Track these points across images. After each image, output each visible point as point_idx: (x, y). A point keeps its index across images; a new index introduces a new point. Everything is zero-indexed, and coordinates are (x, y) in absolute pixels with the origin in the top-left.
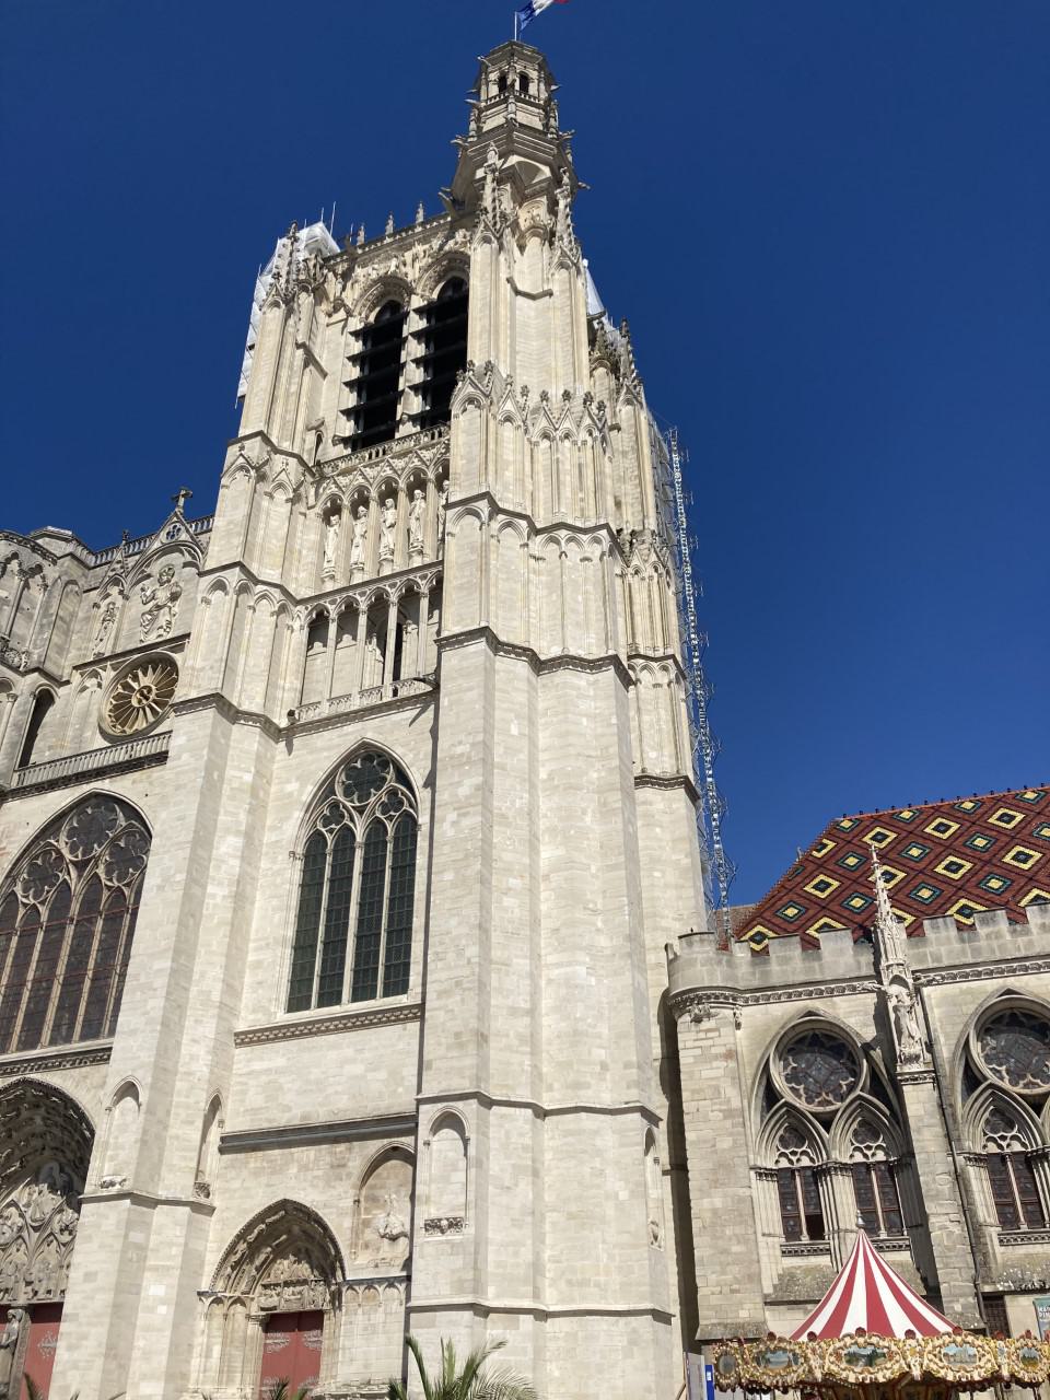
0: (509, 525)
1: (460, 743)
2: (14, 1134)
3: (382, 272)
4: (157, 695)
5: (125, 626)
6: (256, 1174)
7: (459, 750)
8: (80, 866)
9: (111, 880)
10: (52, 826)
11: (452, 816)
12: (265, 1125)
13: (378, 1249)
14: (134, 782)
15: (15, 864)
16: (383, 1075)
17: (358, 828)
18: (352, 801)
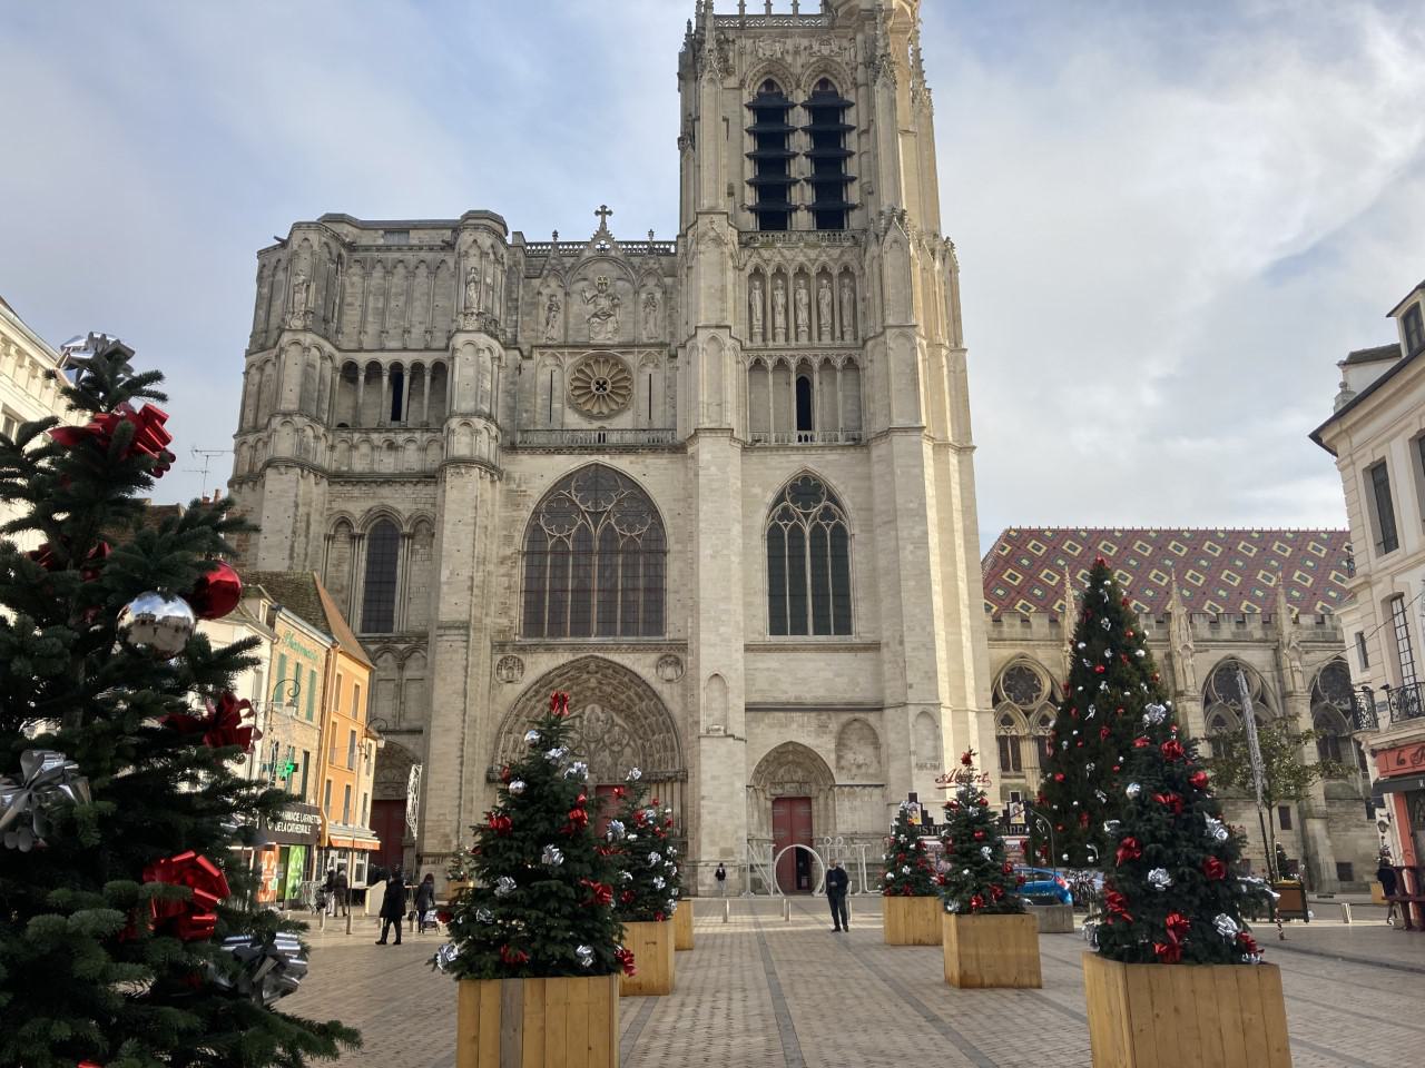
2: (575, 687)
3: (768, 53)
4: (613, 388)
5: (571, 320)
6: (771, 726)
8: (596, 515)
10: (565, 481)
12: (771, 700)
13: (850, 770)
14: (631, 463)
16: (846, 680)
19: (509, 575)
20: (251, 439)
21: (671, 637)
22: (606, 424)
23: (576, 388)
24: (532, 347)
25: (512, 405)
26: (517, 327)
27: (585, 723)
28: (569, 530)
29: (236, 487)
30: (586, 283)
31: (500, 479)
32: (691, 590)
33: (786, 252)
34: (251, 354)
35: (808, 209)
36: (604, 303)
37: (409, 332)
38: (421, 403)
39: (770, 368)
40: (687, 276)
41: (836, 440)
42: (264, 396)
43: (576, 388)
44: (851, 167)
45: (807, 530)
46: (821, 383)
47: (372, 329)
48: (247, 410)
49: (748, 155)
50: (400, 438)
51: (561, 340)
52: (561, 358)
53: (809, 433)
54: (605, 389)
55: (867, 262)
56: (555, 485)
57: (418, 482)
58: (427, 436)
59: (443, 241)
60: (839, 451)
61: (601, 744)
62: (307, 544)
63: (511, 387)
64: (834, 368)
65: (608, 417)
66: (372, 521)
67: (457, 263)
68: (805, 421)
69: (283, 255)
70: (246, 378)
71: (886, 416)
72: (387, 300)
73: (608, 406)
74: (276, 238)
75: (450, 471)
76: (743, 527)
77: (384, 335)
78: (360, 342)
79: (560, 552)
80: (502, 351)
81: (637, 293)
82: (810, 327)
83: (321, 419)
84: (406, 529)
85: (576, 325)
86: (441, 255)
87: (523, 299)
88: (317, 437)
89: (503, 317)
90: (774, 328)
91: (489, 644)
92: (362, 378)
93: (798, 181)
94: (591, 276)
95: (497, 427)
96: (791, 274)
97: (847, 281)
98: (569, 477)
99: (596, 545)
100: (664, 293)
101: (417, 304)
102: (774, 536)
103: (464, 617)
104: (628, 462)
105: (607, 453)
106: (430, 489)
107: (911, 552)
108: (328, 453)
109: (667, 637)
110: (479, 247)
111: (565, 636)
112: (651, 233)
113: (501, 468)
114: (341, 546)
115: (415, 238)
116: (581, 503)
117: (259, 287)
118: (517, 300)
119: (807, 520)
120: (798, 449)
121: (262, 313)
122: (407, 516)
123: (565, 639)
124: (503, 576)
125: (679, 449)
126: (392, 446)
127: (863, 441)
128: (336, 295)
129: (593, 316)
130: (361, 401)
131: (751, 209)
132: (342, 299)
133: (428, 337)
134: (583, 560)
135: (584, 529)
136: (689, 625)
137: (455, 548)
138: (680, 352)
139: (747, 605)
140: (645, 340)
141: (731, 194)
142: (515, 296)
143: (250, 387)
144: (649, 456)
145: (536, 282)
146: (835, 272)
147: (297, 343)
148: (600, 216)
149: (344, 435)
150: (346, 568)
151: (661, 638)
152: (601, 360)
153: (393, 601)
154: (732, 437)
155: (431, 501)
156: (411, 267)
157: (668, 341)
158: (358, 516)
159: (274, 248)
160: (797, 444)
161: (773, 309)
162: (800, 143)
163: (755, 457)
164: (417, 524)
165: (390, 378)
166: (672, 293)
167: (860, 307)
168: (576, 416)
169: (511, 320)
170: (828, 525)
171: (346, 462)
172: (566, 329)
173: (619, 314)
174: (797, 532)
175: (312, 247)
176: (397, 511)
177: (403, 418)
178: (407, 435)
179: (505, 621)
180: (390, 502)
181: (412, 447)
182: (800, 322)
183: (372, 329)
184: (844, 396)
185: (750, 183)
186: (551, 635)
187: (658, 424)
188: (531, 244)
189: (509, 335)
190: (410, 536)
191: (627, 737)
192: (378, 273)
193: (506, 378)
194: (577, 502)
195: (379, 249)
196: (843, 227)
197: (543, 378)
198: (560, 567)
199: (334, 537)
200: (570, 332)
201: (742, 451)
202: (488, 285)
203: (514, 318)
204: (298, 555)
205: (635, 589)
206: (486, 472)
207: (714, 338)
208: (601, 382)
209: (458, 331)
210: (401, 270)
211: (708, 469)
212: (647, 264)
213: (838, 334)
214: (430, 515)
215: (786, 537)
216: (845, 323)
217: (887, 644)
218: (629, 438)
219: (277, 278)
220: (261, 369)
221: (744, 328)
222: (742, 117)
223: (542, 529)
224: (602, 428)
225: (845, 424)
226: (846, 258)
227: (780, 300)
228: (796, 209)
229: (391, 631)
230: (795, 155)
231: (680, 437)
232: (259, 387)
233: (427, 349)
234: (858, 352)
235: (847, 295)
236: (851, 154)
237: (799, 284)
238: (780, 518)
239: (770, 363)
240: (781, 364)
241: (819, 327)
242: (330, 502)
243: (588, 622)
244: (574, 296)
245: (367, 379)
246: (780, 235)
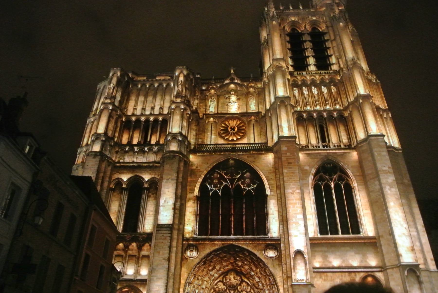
1: (384, 166)
9: (245, 187)
27: (228, 280)
30: (225, 92)
45: (332, 185)
54: (234, 130)
61: (237, 291)
84: (146, 186)
85: (221, 106)
111: (218, 235)
119: (332, 182)
151: (266, 236)
169: (195, 103)
174: (328, 187)
191: (249, 288)
200: (219, 109)
208: (233, 127)
211: (286, 154)
236: (329, 48)
238: (319, 180)
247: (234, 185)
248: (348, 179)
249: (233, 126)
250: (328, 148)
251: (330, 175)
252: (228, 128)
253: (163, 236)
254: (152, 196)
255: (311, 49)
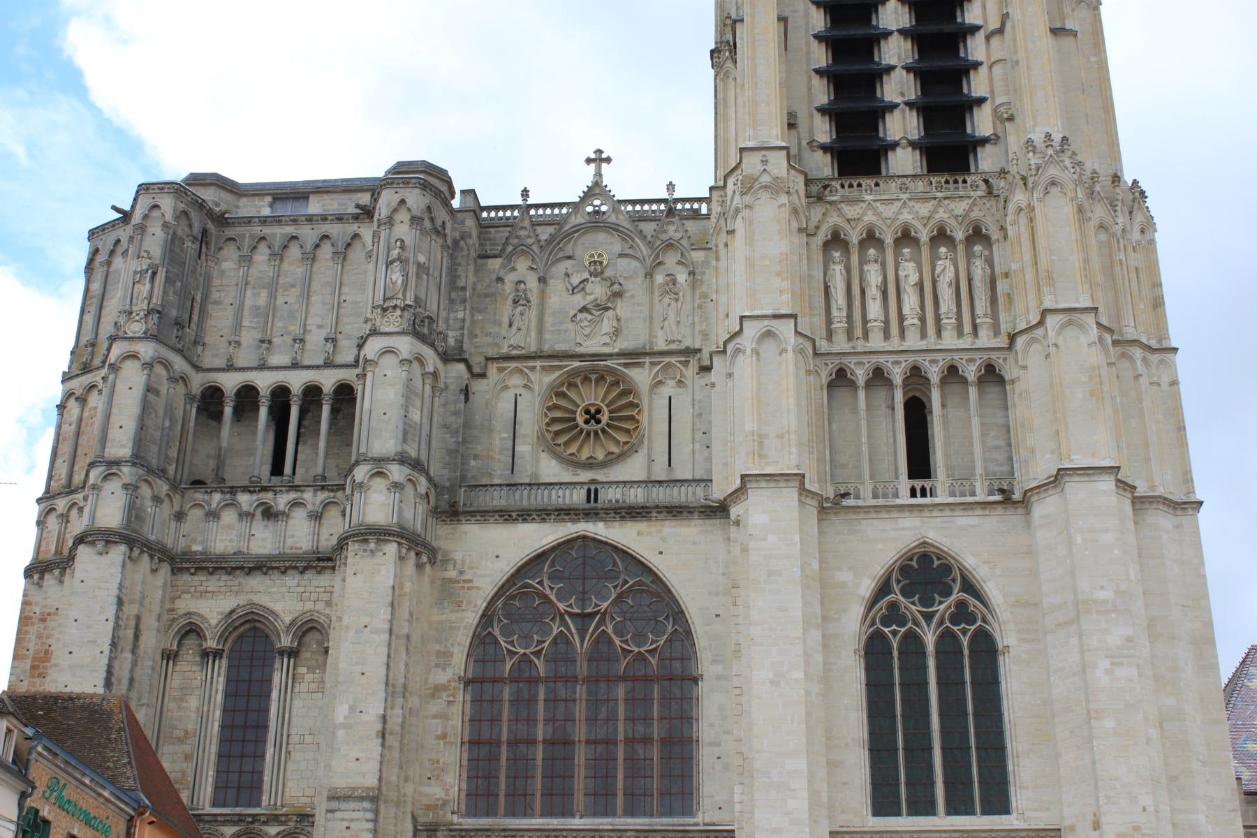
0: (1070, 323)
1: (1102, 588)
4: (611, 418)
5: (549, 320)
7: (1102, 595)
9: (626, 642)
11: (1105, 664)
15: (489, 603)
17: (930, 636)
18: (913, 603)
19: (443, 716)
20: (61, 504)
21: (707, 820)
22: (600, 476)
23: (554, 420)
24: (488, 359)
25: (452, 446)
26: (463, 328)
28: (540, 642)
29: (36, 577)
31: (433, 562)
32: (739, 740)
33: (881, 208)
34: (70, 379)
35: (913, 145)
36: (597, 290)
37: (302, 341)
38: (316, 447)
39: (861, 381)
40: (726, 245)
41: (973, 494)
42: (83, 440)
43: (554, 420)
44: (978, 85)
46: (943, 406)
47: (249, 337)
48: (59, 462)
49: (819, 72)
50: (282, 501)
51: (533, 349)
52: (531, 375)
53: (927, 484)
54: (598, 422)
55: (1009, 218)
56: (519, 570)
57: (305, 569)
58: (322, 496)
59: (358, 206)
60: (979, 512)
62: (135, 663)
63: (453, 418)
64: (964, 381)
65: (604, 464)
66: (236, 628)
67: (376, 235)
68: (920, 464)
69: (123, 233)
70: (61, 414)
71: (1053, 452)
72: (273, 295)
73: (603, 446)
74: (114, 208)
75: (353, 547)
76: (824, 636)
77: (264, 345)
78: (230, 359)
79: (523, 677)
80: (440, 365)
81: (649, 275)
82: (922, 319)
83: (164, 471)
84: (286, 641)
86: (353, 228)
87: (474, 289)
88: (157, 499)
89: (443, 314)
90: (865, 321)
91: (409, 826)
92: (228, 410)
93: (896, 106)
94: (578, 253)
95: (430, 479)
96: (889, 240)
97: (978, 248)
98: (541, 557)
99: (582, 667)
100: (692, 273)
101: (315, 299)
102: (875, 650)
103: (371, 781)
104: (635, 533)
105: (602, 520)
106: (324, 580)
107: (1107, 671)
108: (173, 524)
109: (699, 819)
110: (409, 210)
111: (532, 816)
112: (671, 187)
113: (435, 544)
114: (188, 669)
115: (315, 206)
116: (559, 600)
117: (88, 281)
118: (464, 289)
119: (928, 625)
120: (911, 507)
121: (89, 319)
122: (288, 620)
123: (534, 821)
124: (434, 717)
125: (718, 510)
126: (269, 513)
127: (1017, 496)
128: (197, 289)
129: (581, 311)
130: (224, 444)
131: (825, 148)
132: (206, 295)
133: (330, 346)
134: (562, 692)
135: (563, 639)
136: (737, 798)
137: (359, 669)
138: (717, 361)
139: (832, 765)
140: (661, 345)
141: (791, 126)
142: (461, 283)
143: (65, 427)
144: (667, 523)
145: (495, 264)
146: (959, 235)
147: (134, 356)
148: (593, 166)
149: (199, 496)
150: (193, 702)
151: (692, 821)
152: (594, 377)
153: (263, 756)
154: (803, 490)
155: (325, 597)
156: (309, 247)
157: (697, 346)
158: (214, 622)
159: (113, 224)
160: (905, 499)
161: (863, 292)
162: (896, 52)
163: (838, 525)
164: (301, 638)
165: (270, 408)
166: (704, 273)
167: (1001, 286)
168: (554, 462)
169: (456, 319)
170: (964, 632)
171: (200, 538)
172: (540, 332)
173: (622, 308)
174: (913, 643)
175: (163, 215)
176: (273, 613)
177: (288, 469)
178: (292, 495)
179: (435, 792)
180: (257, 599)
181: (299, 515)
182: (906, 311)
183: (249, 337)
184: (982, 424)
185: (822, 110)
186: (512, 813)
187: (683, 472)
188: (489, 209)
189: (451, 342)
190: (293, 653)
192: (262, 255)
193: (445, 405)
194: (553, 597)
195: (264, 221)
196: (966, 169)
197: (504, 406)
198: (524, 703)
199: (176, 654)
200: (547, 336)
201: (819, 512)
202: (419, 265)
203: (460, 315)
204: (119, 681)
205: (646, 740)
206: (409, 549)
207: (769, 334)
208: (593, 411)
209: (374, 332)
210: (294, 251)
211: (765, 539)
212: (665, 232)
213: (967, 328)
214: (322, 619)
215: (895, 653)
216: (979, 311)
217: (1072, 829)
218: (637, 496)
219: (112, 268)
220: (82, 400)
221: (820, 321)
222: (807, 15)
223: (496, 642)
224: (593, 481)
225: (986, 468)
226: (975, 214)
227: (874, 277)
228: (894, 146)
229: (258, 805)
230: (890, 69)
231: (718, 492)
232: (79, 428)
233: (329, 364)
234: (1002, 355)
235: (979, 269)
236: (976, 65)
237: (902, 255)
238: (886, 621)
239: (861, 375)
240: (879, 377)
241: (938, 319)
242: (173, 600)
243: (567, 794)
244: (551, 282)
245: (238, 413)
246: (868, 182)
247: (588, 636)
248: (989, 617)
249: (594, 405)
250: (928, 500)
251: (927, 601)
252: (575, 413)
253: (348, 828)
254: (309, 677)
255: (904, 72)
